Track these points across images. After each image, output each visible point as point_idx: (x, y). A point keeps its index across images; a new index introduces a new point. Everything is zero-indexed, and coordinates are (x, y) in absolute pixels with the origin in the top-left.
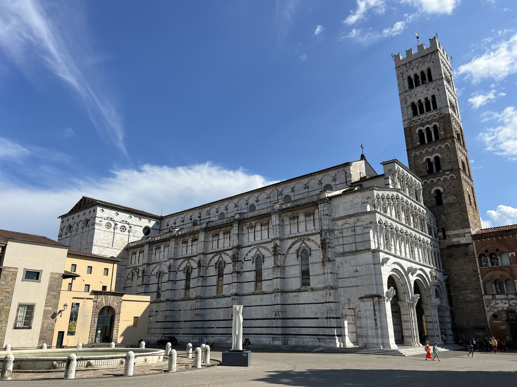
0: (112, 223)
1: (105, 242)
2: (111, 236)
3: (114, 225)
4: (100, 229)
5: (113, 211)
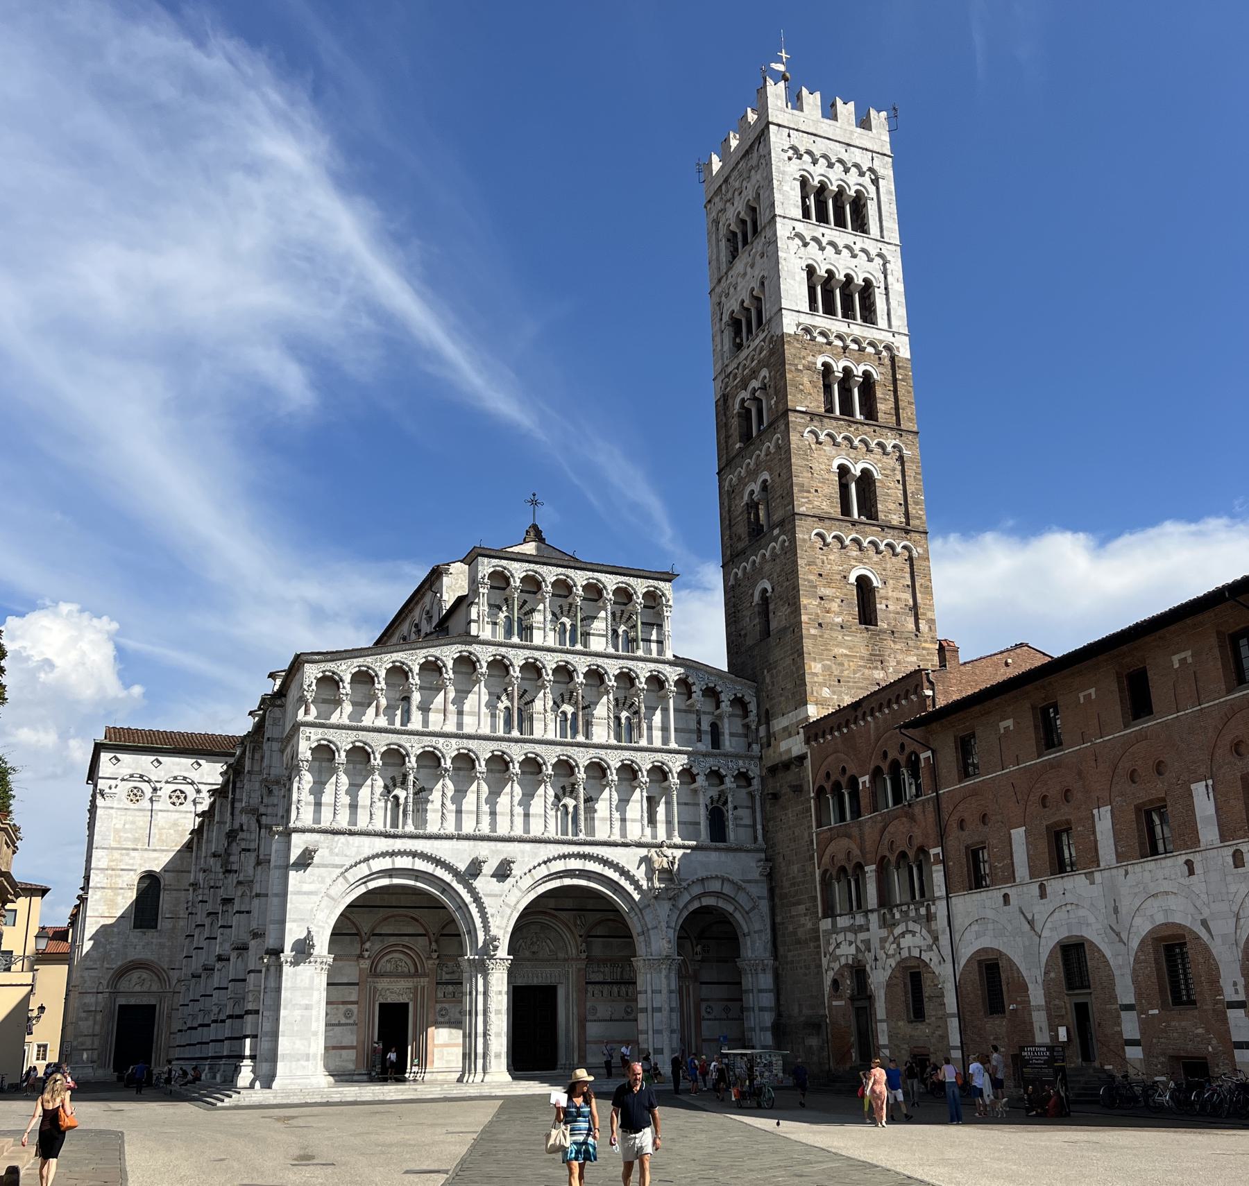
0: (145, 786)
1: (127, 837)
2: (142, 820)
3: (151, 790)
4: (110, 805)
5: (144, 757)
